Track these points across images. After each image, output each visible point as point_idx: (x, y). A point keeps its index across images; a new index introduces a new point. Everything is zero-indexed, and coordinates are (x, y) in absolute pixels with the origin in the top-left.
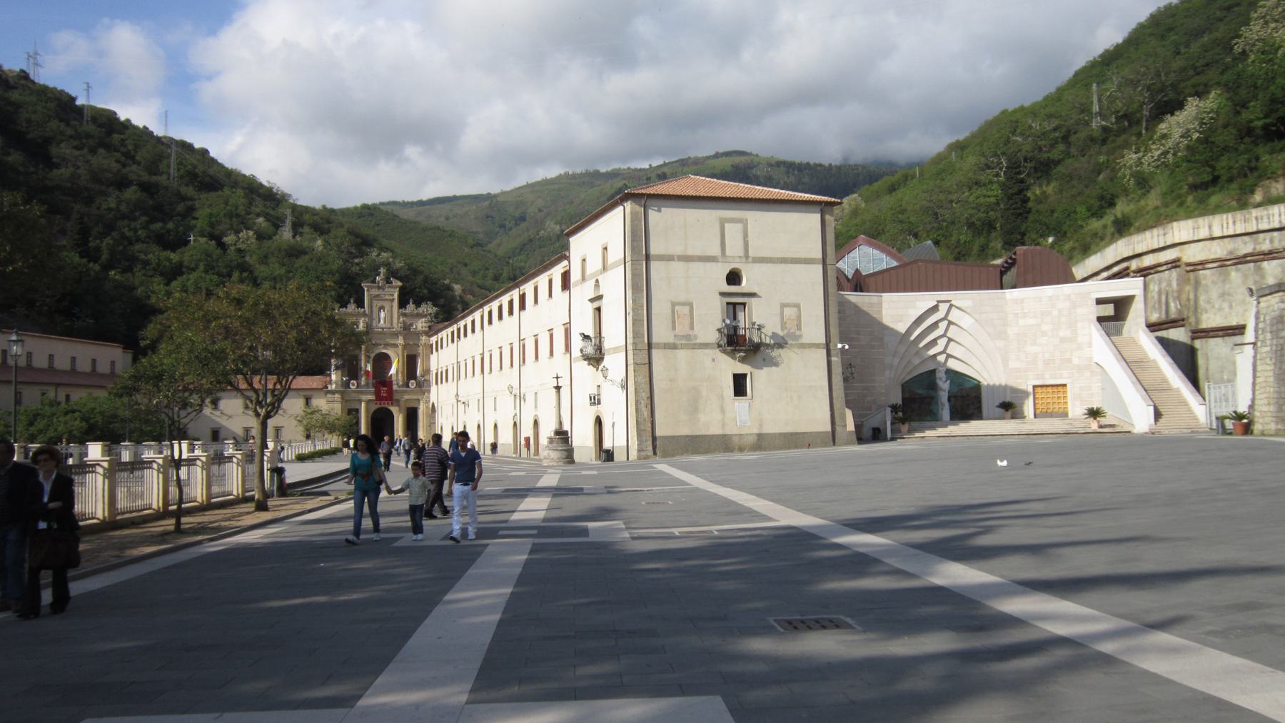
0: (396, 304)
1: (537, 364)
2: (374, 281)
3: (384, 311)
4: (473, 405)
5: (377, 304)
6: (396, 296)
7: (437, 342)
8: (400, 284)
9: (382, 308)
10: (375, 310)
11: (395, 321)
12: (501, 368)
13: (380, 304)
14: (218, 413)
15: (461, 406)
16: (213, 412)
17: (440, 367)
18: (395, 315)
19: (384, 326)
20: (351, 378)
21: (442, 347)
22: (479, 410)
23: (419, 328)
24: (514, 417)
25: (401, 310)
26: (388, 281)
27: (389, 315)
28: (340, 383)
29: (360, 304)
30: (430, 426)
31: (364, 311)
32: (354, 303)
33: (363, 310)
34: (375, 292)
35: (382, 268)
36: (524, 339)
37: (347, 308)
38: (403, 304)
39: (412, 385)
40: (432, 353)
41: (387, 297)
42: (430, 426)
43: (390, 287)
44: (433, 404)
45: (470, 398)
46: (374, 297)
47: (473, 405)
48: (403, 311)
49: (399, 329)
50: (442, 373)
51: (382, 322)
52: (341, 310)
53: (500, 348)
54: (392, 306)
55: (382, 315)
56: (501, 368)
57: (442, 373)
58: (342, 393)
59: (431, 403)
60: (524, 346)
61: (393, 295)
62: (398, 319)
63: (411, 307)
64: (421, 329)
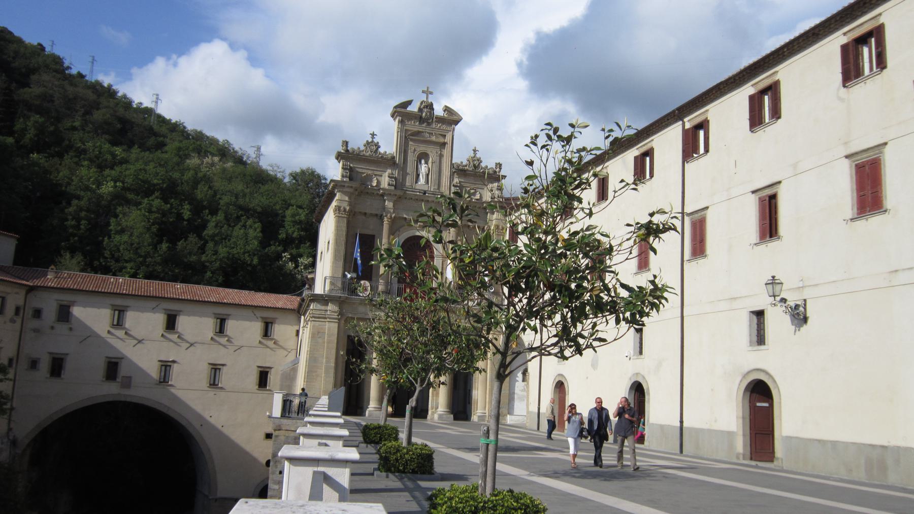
3: (426, 163)
9: (423, 156)
10: (411, 158)
13: (422, 148)
14: (120, 333)
16: (112, 330)
28: (339, 285)
46: (413, 134)
51: (422, 180)
54: (441, 156)
55: (423, 169)
58: (341, 302)
61: (444, 136)
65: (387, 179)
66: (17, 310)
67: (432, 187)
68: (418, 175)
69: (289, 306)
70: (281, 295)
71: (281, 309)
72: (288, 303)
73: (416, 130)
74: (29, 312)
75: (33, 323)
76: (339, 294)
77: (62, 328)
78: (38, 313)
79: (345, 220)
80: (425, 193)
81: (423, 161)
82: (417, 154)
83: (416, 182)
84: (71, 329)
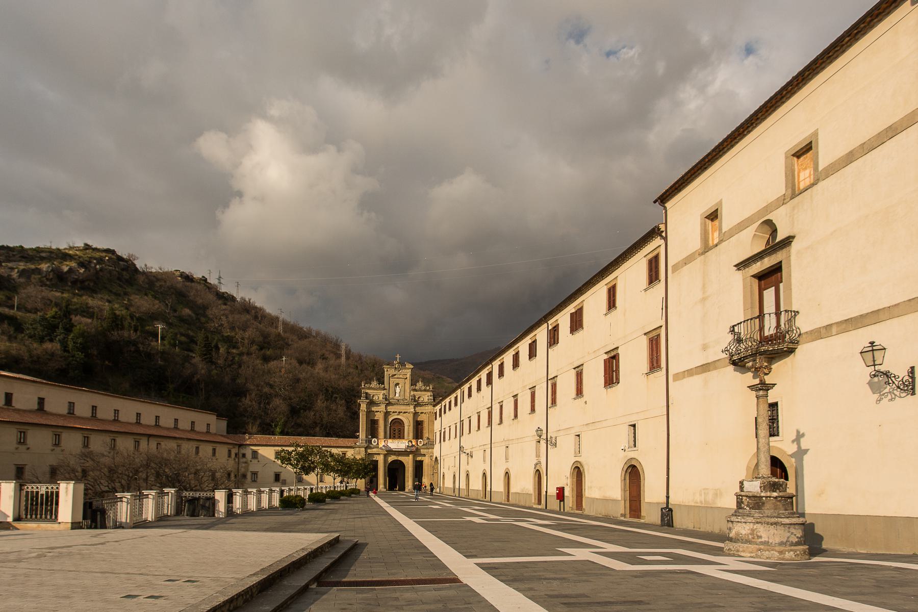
0: (408, 382)
1: (580, 401)
4: (478, 455)
7: (440, 410)
8: (412, 367)
11: (407, 394)
12: (516, 416)
15: (463, 456)
18: (408, 390)
19: (399, 398)
20: (373, 437)
21: (445, 412)
22: (484, 461)
23: (426, 400)
24: (536, 465)
27: (403, 389)
30: (433, 475)
36: (554, 378)
38: (413, 383)
42: (433, 475)
44: (436, 458)
47: (478, 455)
48: (413, 387)
50: (444, 432)
51: (397, 395)
53: (515, 396)
55: (398, 390)
56: (516, 416)
57: (444, 432)
59: (434, 457)
60: (554, 386)
63: (420, 385)
66: (236, 454)
74: (241, 455)
75: (242, 460)
77: (255, 461)
78: (244, 455)
81: (397, 386)
83: (395, 396)
84: (258, 461)
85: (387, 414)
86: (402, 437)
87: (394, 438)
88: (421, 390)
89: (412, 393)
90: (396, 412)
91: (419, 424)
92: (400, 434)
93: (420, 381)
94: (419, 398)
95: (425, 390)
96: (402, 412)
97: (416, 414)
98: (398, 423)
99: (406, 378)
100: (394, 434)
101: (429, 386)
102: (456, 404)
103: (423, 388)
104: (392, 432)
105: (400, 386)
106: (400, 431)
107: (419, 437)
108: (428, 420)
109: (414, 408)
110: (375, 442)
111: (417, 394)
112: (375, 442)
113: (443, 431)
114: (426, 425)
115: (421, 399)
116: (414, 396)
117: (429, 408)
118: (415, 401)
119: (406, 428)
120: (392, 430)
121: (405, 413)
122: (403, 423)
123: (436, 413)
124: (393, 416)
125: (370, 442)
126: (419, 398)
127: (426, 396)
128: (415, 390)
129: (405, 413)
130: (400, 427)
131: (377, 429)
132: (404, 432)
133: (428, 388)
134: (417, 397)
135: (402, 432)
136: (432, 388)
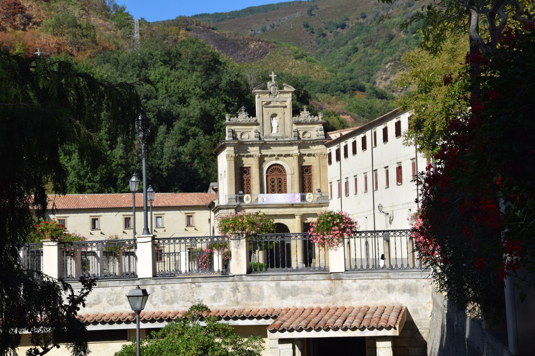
0: (289, 111)
2: (265, 88)
5: (268, 112)
6: (289, 103)
9: (274, 115)
10: (267, 117)
11: (288, 130)
17: (343, 177)
25: (294, 117)
26: (281, 88)
27: (282, 120)
29: (252, 112)
31: (256, 121)
32: (245, 111)
33: (254, 118)
34: (266, 98)
35: (273, 73)
37: (237, 117)
38: (296, 112)
39: (310, 198)
40: (330, 162)
41: (278, 104)
43: (281, 93)
45: (394, 208)
46: (266, 104)
48: (296, 118)
49: (293, 139)
50: (347, 184)
51: (274, 131)
52: (232, 119)
57: (347, 184)
62: (292, 127)
63: (305, 115)
64: (317, 138)
65: (254, 133)
67: (280, 134)
68: (272, 128)
69: (202, 204)
70: (193, 193)
71: (197, 206)
72: (200, 200)
73: (269, 100)
76: (234, 203)
79: (233, 162)
80: (277, 139)
81: (274, 118)
82: (270, 114)
83: (271, 132)
85: (261, 160)
86: (283, 189)
87: (273, 191)
88: (306, 123)
89: (295, 127)
90: (274, 155)
91: (307, 171)
92: (280, 186)
93: (305, 109)
94: (304, 133)
95: (313, 123)
96: (281, 155)
97: (301, 157)
98: (277, 169)
99: (285, 107)
100: (273, 186)
101: (317, 115)
102: (364, 147)
103: (310, 119)
104: (269, 185)
105: (278, 117)
106: (280, 182)
107: (307, 189)
108: (318, 164)
109: (299, 149)
110: (247, 199)
111: (302, 128)
112: (247, 199)
113: (344, 181)
114: (315, 172)
115: (307, 135)
116: (298, 132)
117: (320, 149)
118: (299, 138)
119: (289, 178)
120: (269, 181)
121: (287, 156)
122: (284, 170)
123: (330, 155)
124: (269, 161)
125: (241, 199)
126: (304, 133)
127: (314, 130)
128: (298, 123)
129: (287, 156)
130: (280, 177)
131: (249, 181)
132: (285, 183)
133: (316, 118)
134: (301, 133)
135: (283, 184)
136: (322, 119)
